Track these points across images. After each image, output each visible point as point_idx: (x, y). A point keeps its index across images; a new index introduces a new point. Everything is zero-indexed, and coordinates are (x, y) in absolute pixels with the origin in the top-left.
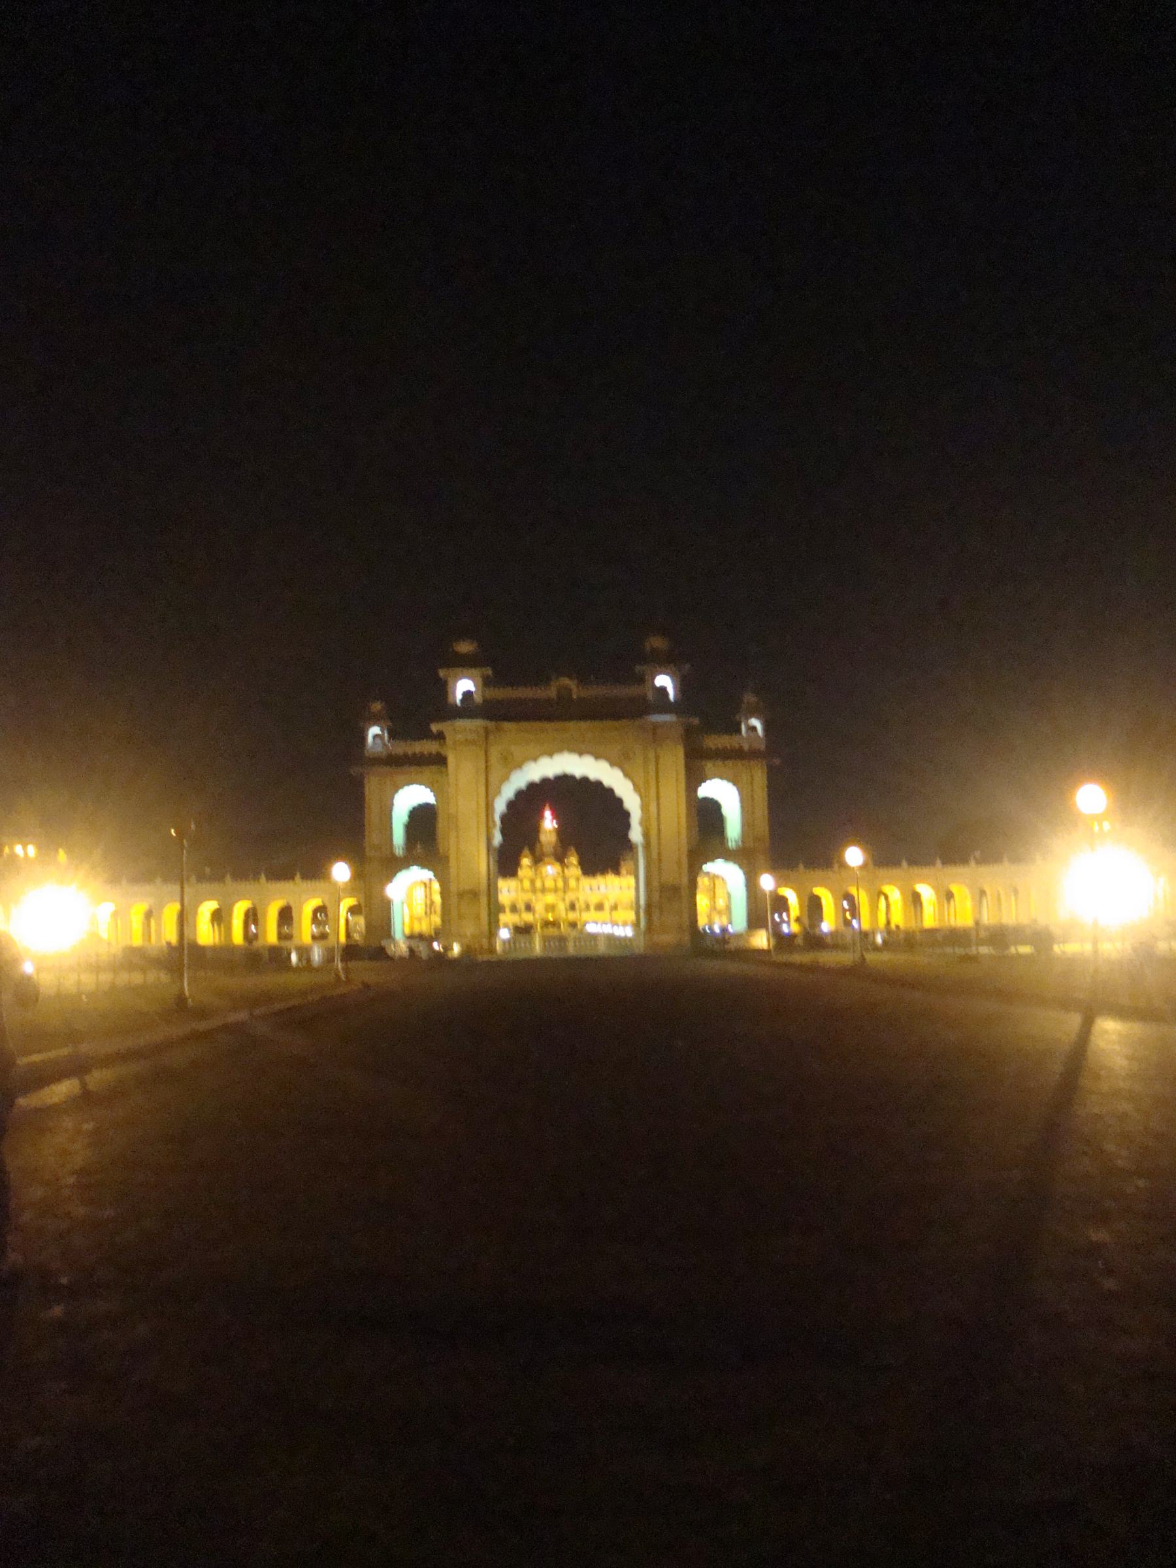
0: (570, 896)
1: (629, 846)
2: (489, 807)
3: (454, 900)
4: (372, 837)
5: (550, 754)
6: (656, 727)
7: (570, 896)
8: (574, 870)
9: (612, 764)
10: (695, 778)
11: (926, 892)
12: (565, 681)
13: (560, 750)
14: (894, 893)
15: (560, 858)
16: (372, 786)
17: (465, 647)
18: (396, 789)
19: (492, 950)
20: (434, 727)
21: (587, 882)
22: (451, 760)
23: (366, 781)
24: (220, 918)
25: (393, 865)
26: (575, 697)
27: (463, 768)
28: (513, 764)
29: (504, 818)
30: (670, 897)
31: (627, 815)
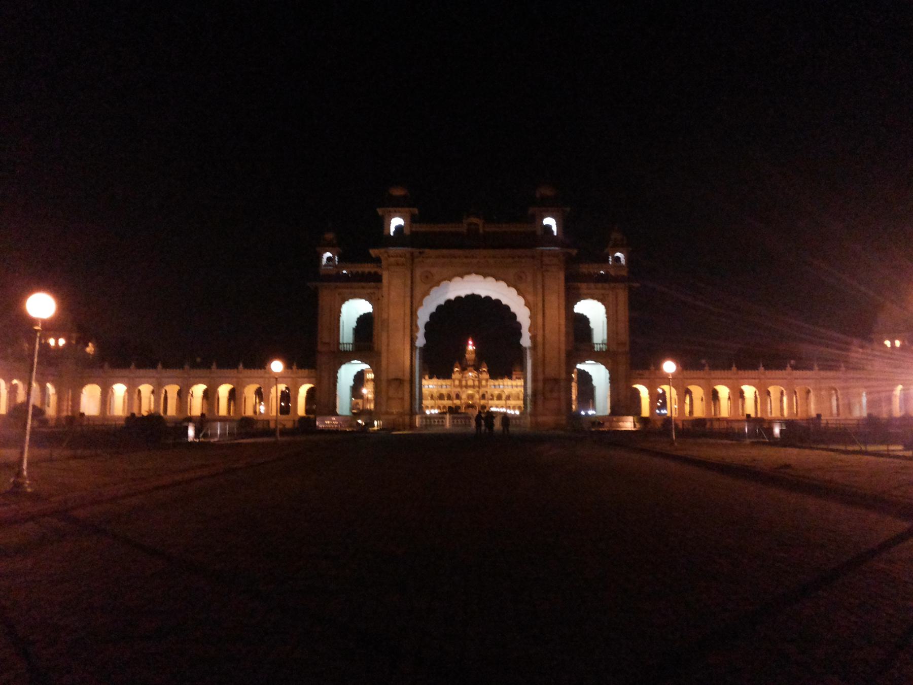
0: (482, 391)
1: (521, 350)
3: (384, 384)
5: (462, 276)
6: (542, 254)
7: (482, 391)
8: (485, 376)
9: (509, 285)
10: (573, 297)
11: (723, 391)
12: (474, 220)
13: (469, 273)
14: (698, 391)
15: (477, 368)
16: (325, 297)
17: (398, 192)
18: (344, 300)
19: (412, 426)
20: (373, 252)
22: (385, 276)
26: (481, 231)
27: (394, 285)
28: (433, 282)
29: (427, 326)
30: (557, 387)
31: (519, 326)
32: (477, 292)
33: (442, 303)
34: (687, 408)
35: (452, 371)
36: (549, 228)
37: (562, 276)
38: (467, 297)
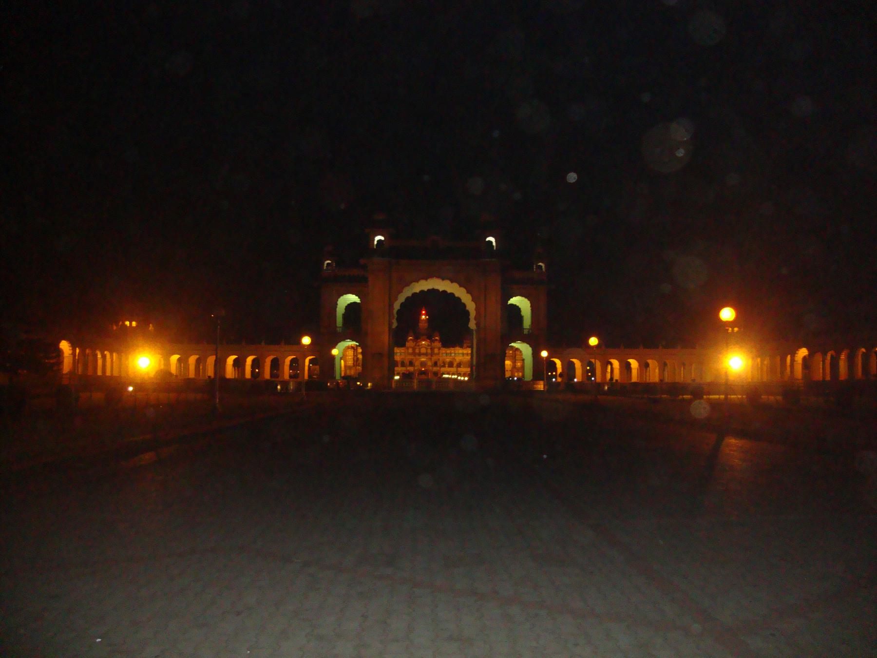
0: (434, 358)
1: (469, 331)
2: (391, 306)
5: (426, 279)
7: (434, 358)
8: (438, 344)
9: (461, 286)
11: (634, 363)
14: (616, 363)
15: (430, 337)
20: (362, 261)
21: (443, 350)
30: (489, 361)
31: (467, 313)
32: (436, 287)
33: (410, 295)
34: (608, 376)
35: (406, 340)
38: (428, 290)
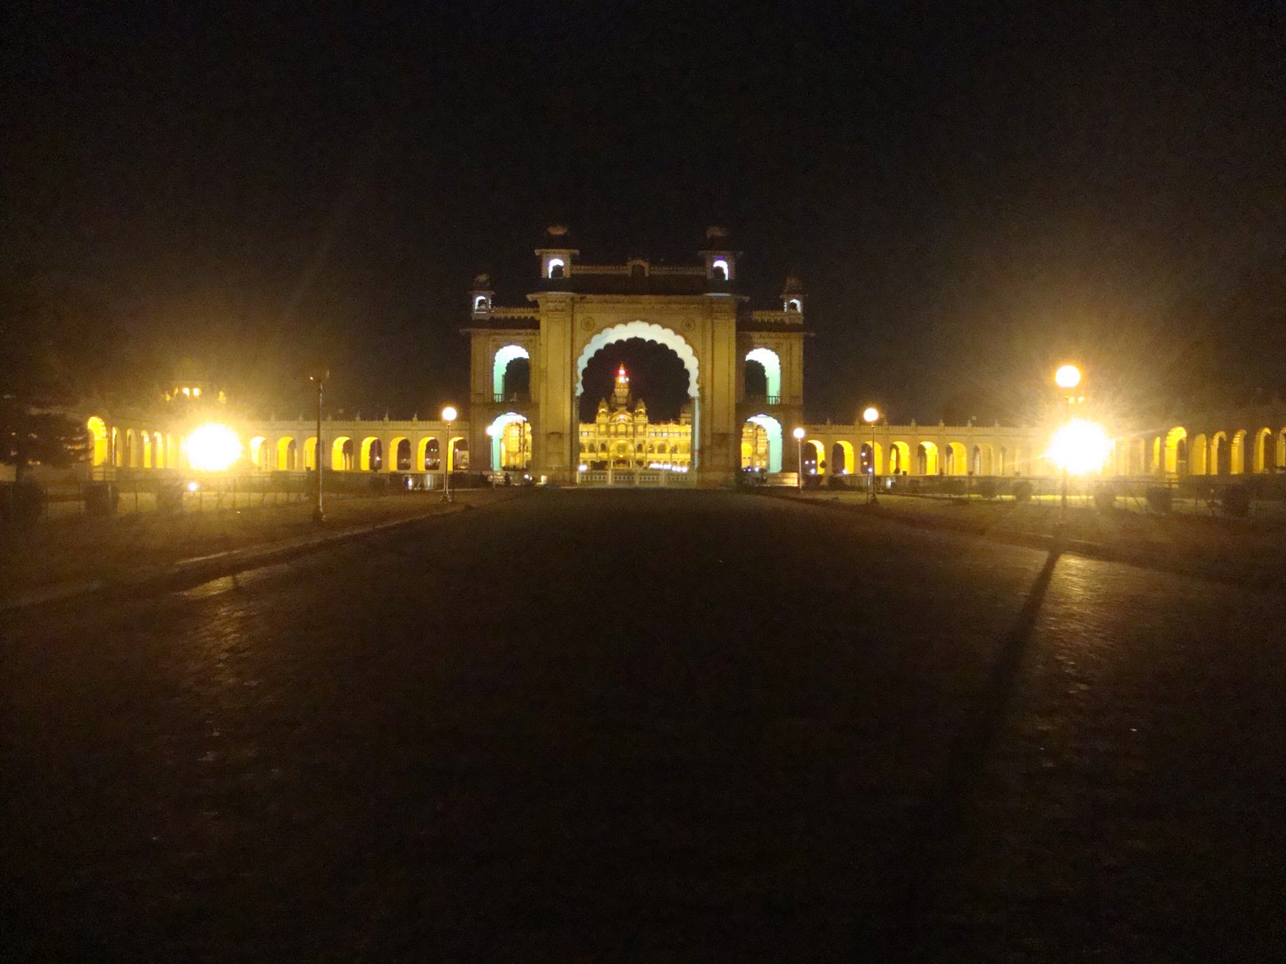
0: (639, 439)
1: (688, 400)
3: (543, 440)
4: (476, 384)
5: (625, 323)
6: (712, 301)
7: (639, 439)
8: (643, 419)
10: (744, 345)
11: (931, 448)
13: (633, 320)
14: (904, 448)
16: (478, 344)
17: (558, 231)
18: (499, 347)
19: (572, 482)
20: (530, 297)
21: (652, 428)
23: (473, 341)
24: (350, 449)
25: (494, 409)
27: (553, 332)
28: (594, 329)
29: (585, 372)
30: (719, 443)
31: (687, 373)
32: (639, 336)
36: (720, 270)
37: (733, 321)
38: (630, 340)
